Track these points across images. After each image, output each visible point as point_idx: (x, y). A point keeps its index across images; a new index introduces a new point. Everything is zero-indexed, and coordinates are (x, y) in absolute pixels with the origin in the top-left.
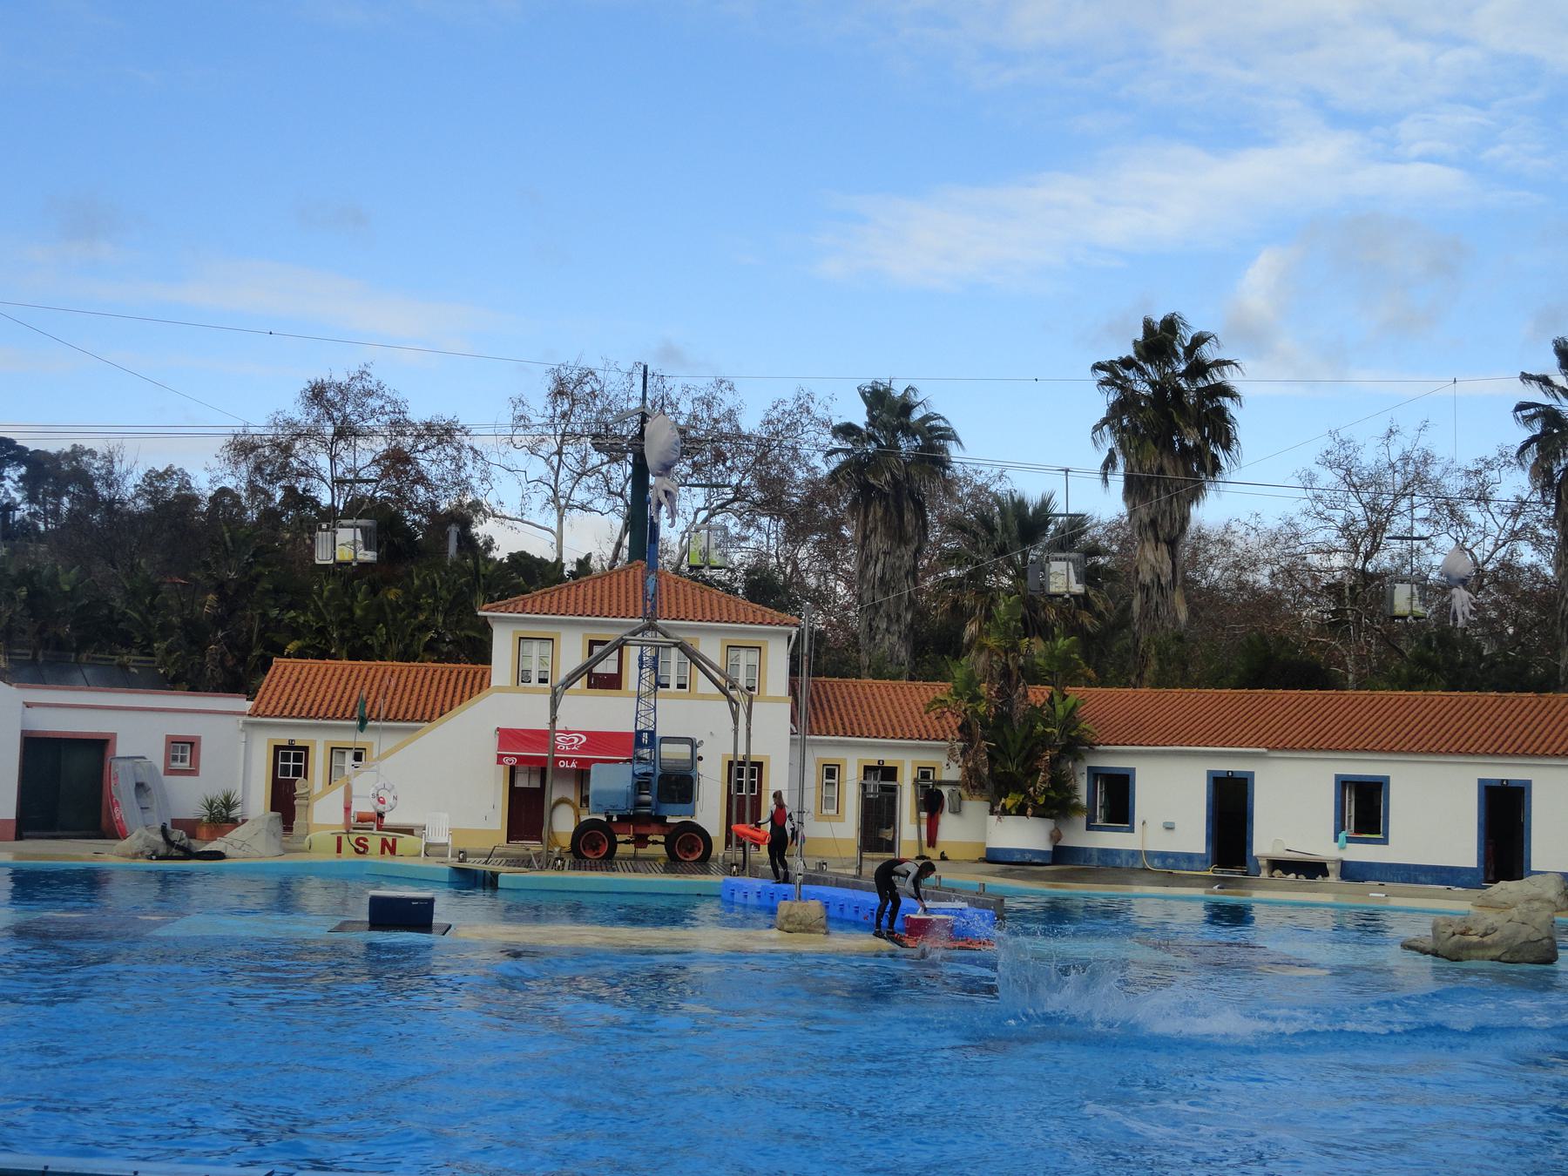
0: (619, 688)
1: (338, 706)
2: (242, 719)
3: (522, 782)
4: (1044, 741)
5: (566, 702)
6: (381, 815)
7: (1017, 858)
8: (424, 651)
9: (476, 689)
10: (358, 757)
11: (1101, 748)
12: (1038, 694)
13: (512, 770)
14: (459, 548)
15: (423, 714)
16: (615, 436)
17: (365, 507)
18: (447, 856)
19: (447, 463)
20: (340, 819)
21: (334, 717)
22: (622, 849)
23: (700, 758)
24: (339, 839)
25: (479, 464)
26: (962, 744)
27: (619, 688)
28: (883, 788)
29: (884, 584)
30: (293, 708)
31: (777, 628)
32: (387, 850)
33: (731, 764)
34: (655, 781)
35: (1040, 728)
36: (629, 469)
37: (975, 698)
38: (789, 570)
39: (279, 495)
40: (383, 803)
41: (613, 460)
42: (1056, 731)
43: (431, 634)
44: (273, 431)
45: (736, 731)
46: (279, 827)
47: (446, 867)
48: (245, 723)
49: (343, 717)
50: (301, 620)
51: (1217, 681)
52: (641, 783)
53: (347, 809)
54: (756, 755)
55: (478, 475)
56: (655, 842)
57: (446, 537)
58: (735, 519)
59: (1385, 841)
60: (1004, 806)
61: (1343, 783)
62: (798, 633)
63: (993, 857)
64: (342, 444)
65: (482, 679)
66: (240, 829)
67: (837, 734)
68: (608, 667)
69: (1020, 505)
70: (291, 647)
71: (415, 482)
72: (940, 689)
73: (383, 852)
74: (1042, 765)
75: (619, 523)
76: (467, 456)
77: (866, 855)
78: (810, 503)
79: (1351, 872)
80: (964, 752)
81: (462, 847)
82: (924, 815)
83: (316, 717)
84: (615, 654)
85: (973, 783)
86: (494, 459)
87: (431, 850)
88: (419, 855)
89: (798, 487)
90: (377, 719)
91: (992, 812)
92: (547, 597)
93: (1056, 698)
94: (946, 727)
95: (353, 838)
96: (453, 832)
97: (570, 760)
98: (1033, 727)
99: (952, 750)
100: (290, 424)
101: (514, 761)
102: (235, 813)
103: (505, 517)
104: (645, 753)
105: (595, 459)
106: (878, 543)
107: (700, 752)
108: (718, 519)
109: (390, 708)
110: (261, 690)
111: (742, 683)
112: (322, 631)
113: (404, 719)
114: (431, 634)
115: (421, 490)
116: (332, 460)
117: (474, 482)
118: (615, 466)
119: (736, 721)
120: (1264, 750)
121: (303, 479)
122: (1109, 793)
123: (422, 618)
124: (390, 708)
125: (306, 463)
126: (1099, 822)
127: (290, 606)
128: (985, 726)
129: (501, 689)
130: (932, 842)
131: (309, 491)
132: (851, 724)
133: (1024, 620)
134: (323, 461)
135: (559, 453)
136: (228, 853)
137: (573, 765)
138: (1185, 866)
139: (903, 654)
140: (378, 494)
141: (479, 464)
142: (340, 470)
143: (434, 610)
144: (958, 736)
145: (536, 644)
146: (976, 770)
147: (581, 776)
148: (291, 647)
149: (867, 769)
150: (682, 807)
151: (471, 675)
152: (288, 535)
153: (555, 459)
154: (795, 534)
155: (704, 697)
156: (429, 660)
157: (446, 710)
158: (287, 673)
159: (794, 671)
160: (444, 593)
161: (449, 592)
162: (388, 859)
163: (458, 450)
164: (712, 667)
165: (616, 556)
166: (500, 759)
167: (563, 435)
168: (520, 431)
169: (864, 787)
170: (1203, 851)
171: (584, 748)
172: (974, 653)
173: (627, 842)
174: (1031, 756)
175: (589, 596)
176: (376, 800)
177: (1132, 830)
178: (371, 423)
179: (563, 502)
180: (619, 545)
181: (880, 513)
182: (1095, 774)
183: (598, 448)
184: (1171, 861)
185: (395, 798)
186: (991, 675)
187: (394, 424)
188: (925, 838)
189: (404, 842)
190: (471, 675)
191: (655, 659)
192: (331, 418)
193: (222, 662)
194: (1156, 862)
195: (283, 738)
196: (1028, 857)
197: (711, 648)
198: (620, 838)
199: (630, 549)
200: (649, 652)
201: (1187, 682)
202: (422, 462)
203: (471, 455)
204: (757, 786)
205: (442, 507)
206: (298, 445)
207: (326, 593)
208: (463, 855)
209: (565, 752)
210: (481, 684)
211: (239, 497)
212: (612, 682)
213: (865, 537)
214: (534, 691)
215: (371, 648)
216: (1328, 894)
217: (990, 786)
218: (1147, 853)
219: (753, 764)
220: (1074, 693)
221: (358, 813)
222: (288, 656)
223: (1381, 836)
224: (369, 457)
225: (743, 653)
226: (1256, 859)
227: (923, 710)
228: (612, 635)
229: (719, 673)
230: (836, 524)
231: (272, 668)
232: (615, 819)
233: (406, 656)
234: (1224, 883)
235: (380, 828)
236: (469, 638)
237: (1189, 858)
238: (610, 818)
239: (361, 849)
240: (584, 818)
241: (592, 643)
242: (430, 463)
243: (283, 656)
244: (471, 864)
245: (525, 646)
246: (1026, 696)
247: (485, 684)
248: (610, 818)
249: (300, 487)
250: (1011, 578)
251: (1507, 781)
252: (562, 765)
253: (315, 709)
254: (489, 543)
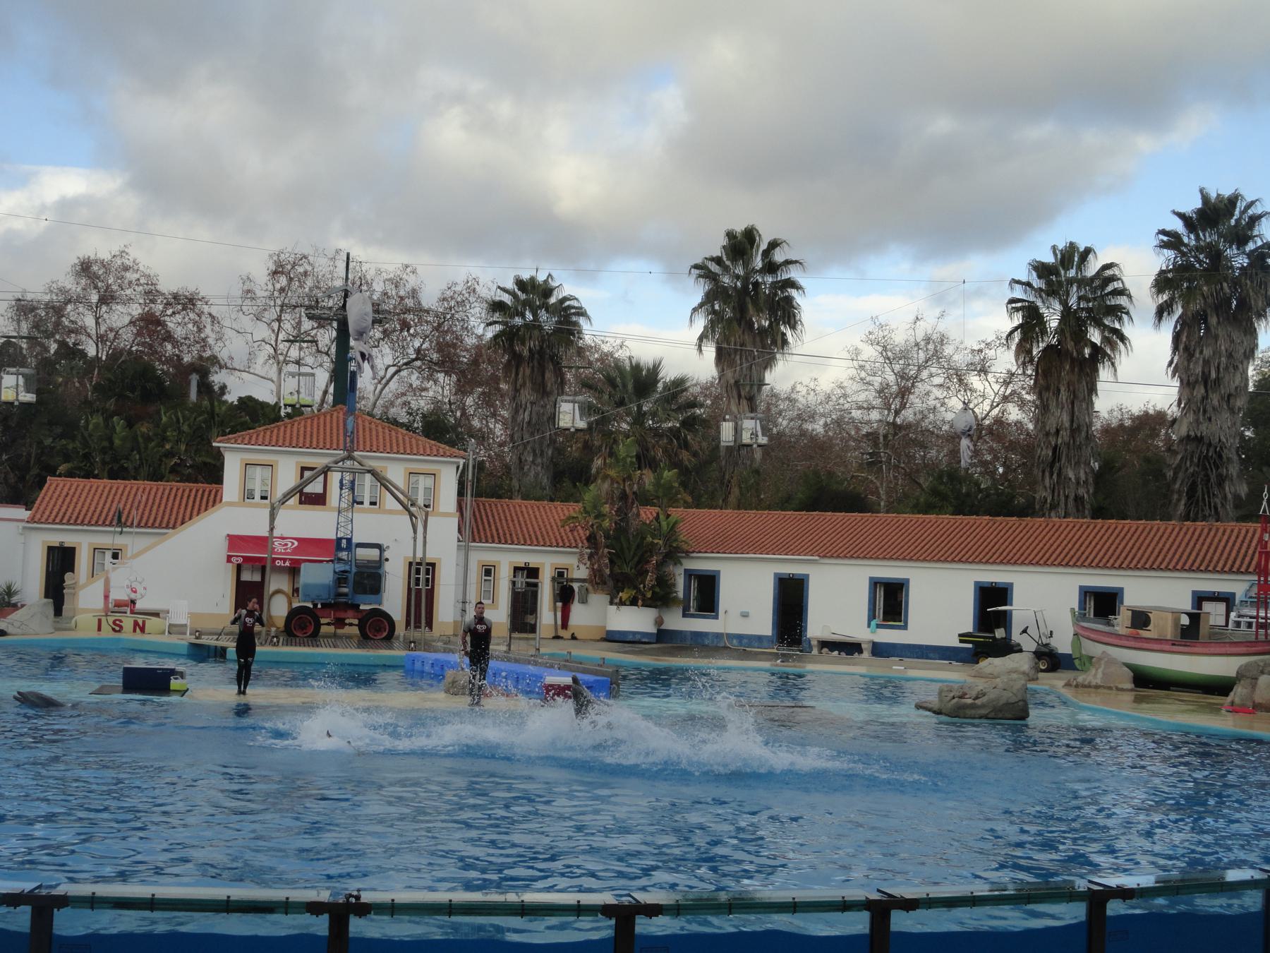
0: (324, 503)
1: (100, 515)
2: (21, 525)
3: (246, 576)
4: (651, 549)
5: (283, 515)
6: (133, 602)
7: (630, 638)
8: (170, 472)
9: (211, 503)
10: (115, 556)
11: (695, 555)
12: (647, 514)
13: (239, 568)
14: (199, 392)
15: (168, 522)
16: (323, 308)
17: (123, 358)
18: (185, 634)
19: (190, 326)
20: (100, 604)
21: (96, 524)
22: (324, 629)
23: (387, 560)
24: (100, 621)
25: (216, 328)
26: (589, 551)
27: (324, 503)
28: (528, 584)
29: (534, 426)
30: (63, 517)
31: (449, 459)
32: (138, 630)
33: (410, 564)
34: (351, 577)
35: (649, 539)
36: (334, 334)
37: (600, 516)
38: (458, 414)
39: (53, 347)
40: (135, 592)
41: (320, 326)
42: (661, 542)
43: (175, 460)
44: (47, 298)
45: (415, 541)
46: (51, 611)
47: (185, 643)
48: (24, 528)
49: (104, 524)
50: (70, 447)
51: (785, 503)
52: (341, 579)
53: (106, 597)
54: (431, 556)
55: (213, 336)
56: (351, 625)
57: (189, 383)
58: (416, 375)
59: (905, 627)
60: (621, 598)
61: (875, 583)
62: (464, 464)
63: (613, 638)
64: (104, 308)
65: (215, 496)
66: (20, 612)
67: (493, 542)
68: (315, 487)
69: (637, 368)
70: (63, 468)
71: (164, 340)
72: (573, 509)
73: (135, 631)
74: (650, 567)
75: (323, 377)
76: (206, 320)
77: (516, 635)
78: (475, 362)
79: (879, 650)
80: (591, 557)
81: (200, 626)
82: (559, 604)
83: (82, 523)
84: (321, 478)
85: (597, 581)
86: (227, 323)
87: (174, 629)
88: (163, 633)
89: (467, 350)
90: (132, 526)
91: (611, 603)
92: (268, 433)
93: (662, 517)
94: (578, 538)
95: (111, 620)
96: (193, 616)
97: (285, 560)
98: (645, 538)
99: (581, 555)
100: (62, 291)
101: (240, 560)
102: (14, 600)
103: (235, 369)
104: (344, 555)
105: (307, 325)
106: (527, 395)
107: (386, 554)
108: (404, 373)
109: (142, 517)
110: (38, 502)
111: (421, 502)
112: (87, 457)
113: (153, 526)
114: (175, 460)
115: (169, 347)
116: (97, 319)
117: (211, 341)
118: (322, 331)
119: (415, 531)
120: (817, 558)
121: (73, 335)
122: (700, 590)
123: (168, 447)
124: (142, 517)
125: (72, 322)
126: (692, 611)
127: (61, 436)
128: (607, 537)
129: (230, 504)
130: (565, 625)
131: (78, 344)
132: (505, 534)
133: (638, 457)
134: (89, 321)
135: (279, 320)
136: (10, 630)
137: (287, 564)
138: (756, 644)
139: (545, 481)
140: (134, 349)
141: (216, 328)
142: (103, 329)
143: (178, 441)
144: (587, 545)
145: (259, 469)
146: (600, 570)
147: (294, 571)
148: (63, 468)
149: (516, 569)
150: (372, 597)
151: (206, 493)
152: (61, 380)
153: (275, 325)
154: (462, 388)
155: (391, 512)
156: (173, 480)
157: (187, 519)
158: (59, 489)
159: (461, 493)
160: (185, 428)
161: (189, 425)
162: (139, 636)
163: (199, 315)
164: (397, 489)
165: (323, 401)
166: (229, 559)
167: (282, 306)
168: (248, 302)
169: (514, 583)
171: (295, 551)
172: (599, 481)
173: (328, 624)
174: (643, 560)
175: (302, 432)
176: (129, 591)
177: (716, 617)
178: (128, 292)
179: (281, 358)
180: (325, 392)
181: (528, 372)
182: (689, 574)
183: (310, 317)
184: (745, 641)
185: (145, 588)
186: (612, 498)
187: (148, 293)
188: (559, 622)
189: (152, 623)
190: (206, 493)
191: (353, 482)
192: (96, 287)
193: (5, 479)
194: (735, 641)
195: (56, 539)
196: (638, 637)
197: (396, 472)
198: (323, 621)
199: (335, 395)
200: (348, 477)
201: (759, 506)
202: (169, 324)
203: (209, 320)
204: (431, 582)
205: (185, 360)
206: (69, 307)
207: (91, 427)
208: (199, 633)
209: (281, 553)
210: (215, 500)
211: (21, 348)
212: (318, 500)
213: (517, 391)
214: (257, 506)
215: (126, 469)
216: (862, 667)
217: (611, 583)
219: (428, 564)
220: (676, 513)
221: (115, 600)
222: (60, 476)
223: (902, 624)
224: (127, 320)
225: (422, 477)
226: (809, 641)
227: (559, 524)
228: (319, 462)
229: (402, 493)
230: (495, 380)
231: (47, 485)
232: (319, 606)
233: (156, 476)
234: (785, 658)
235: (132, 612)
236: (205, 464)
237: (760, 639)
238: (315, 605)
239: (117, 628)
240: (295, 605)
241: (303, 469)
242: (177, 324)
243: (54, 475)
244: (205, 640)
245: (250, 470)
246: (638, 515)
247: (218, 497)
248: (315, 605)
249: (71, 341)
250: (628, 423)
252: (278, 563)
253: (81, 518)
254: (223, 388)
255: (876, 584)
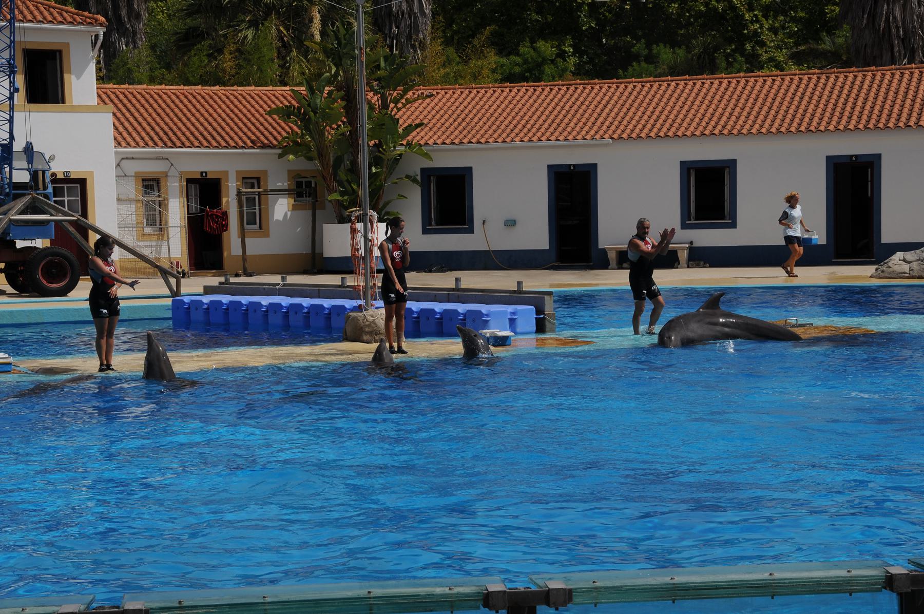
59: (733, 225)
61: (688, 169)
149: (189, 181)
170: (547, 247)
177: (471, 231)
218: (493, 251)
226: (604, 251)
251: (856, 156)
255: (689, 170)
